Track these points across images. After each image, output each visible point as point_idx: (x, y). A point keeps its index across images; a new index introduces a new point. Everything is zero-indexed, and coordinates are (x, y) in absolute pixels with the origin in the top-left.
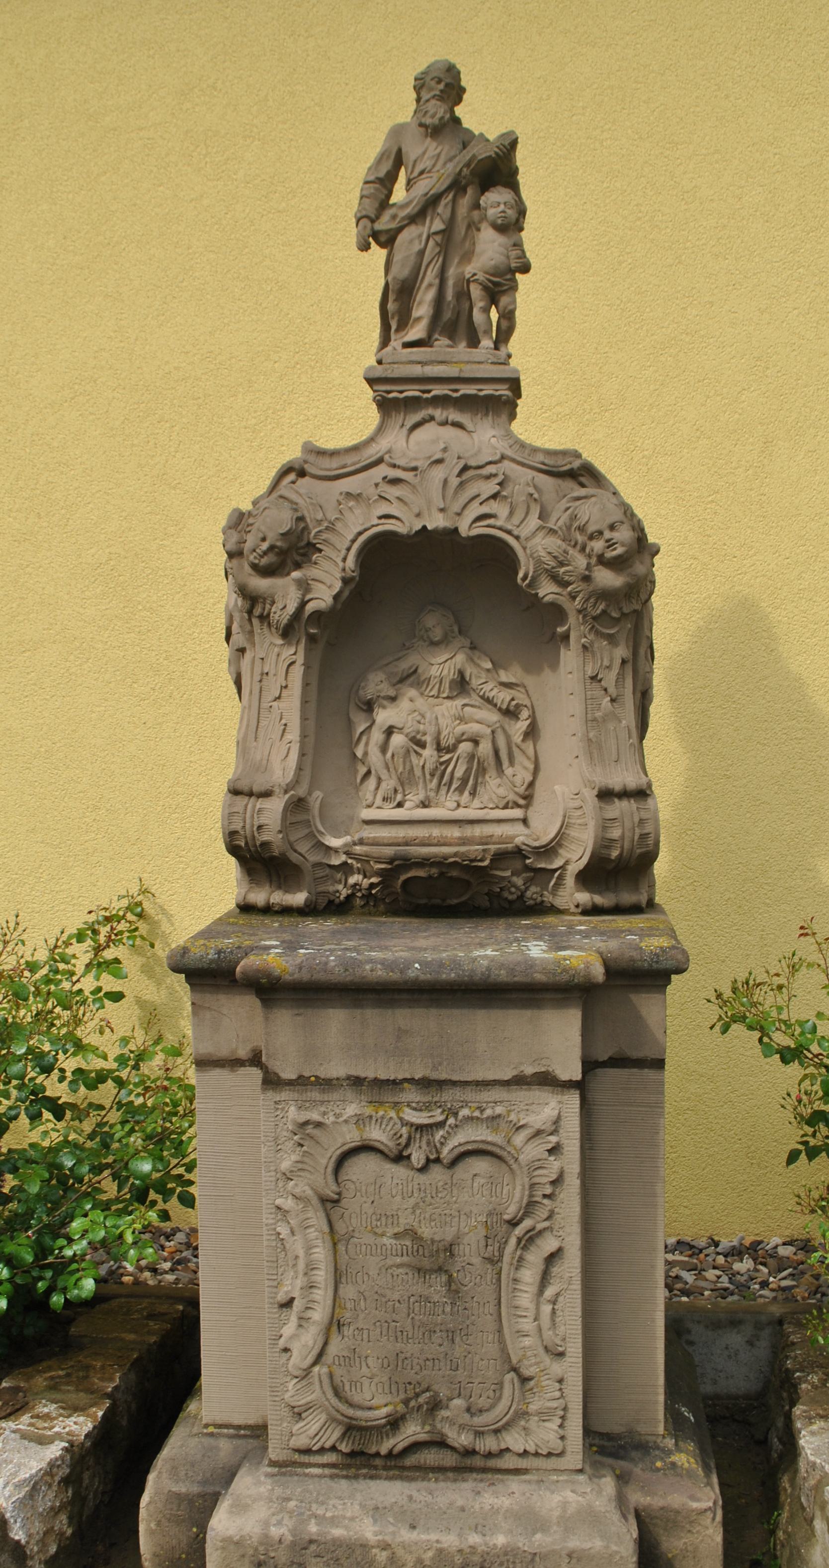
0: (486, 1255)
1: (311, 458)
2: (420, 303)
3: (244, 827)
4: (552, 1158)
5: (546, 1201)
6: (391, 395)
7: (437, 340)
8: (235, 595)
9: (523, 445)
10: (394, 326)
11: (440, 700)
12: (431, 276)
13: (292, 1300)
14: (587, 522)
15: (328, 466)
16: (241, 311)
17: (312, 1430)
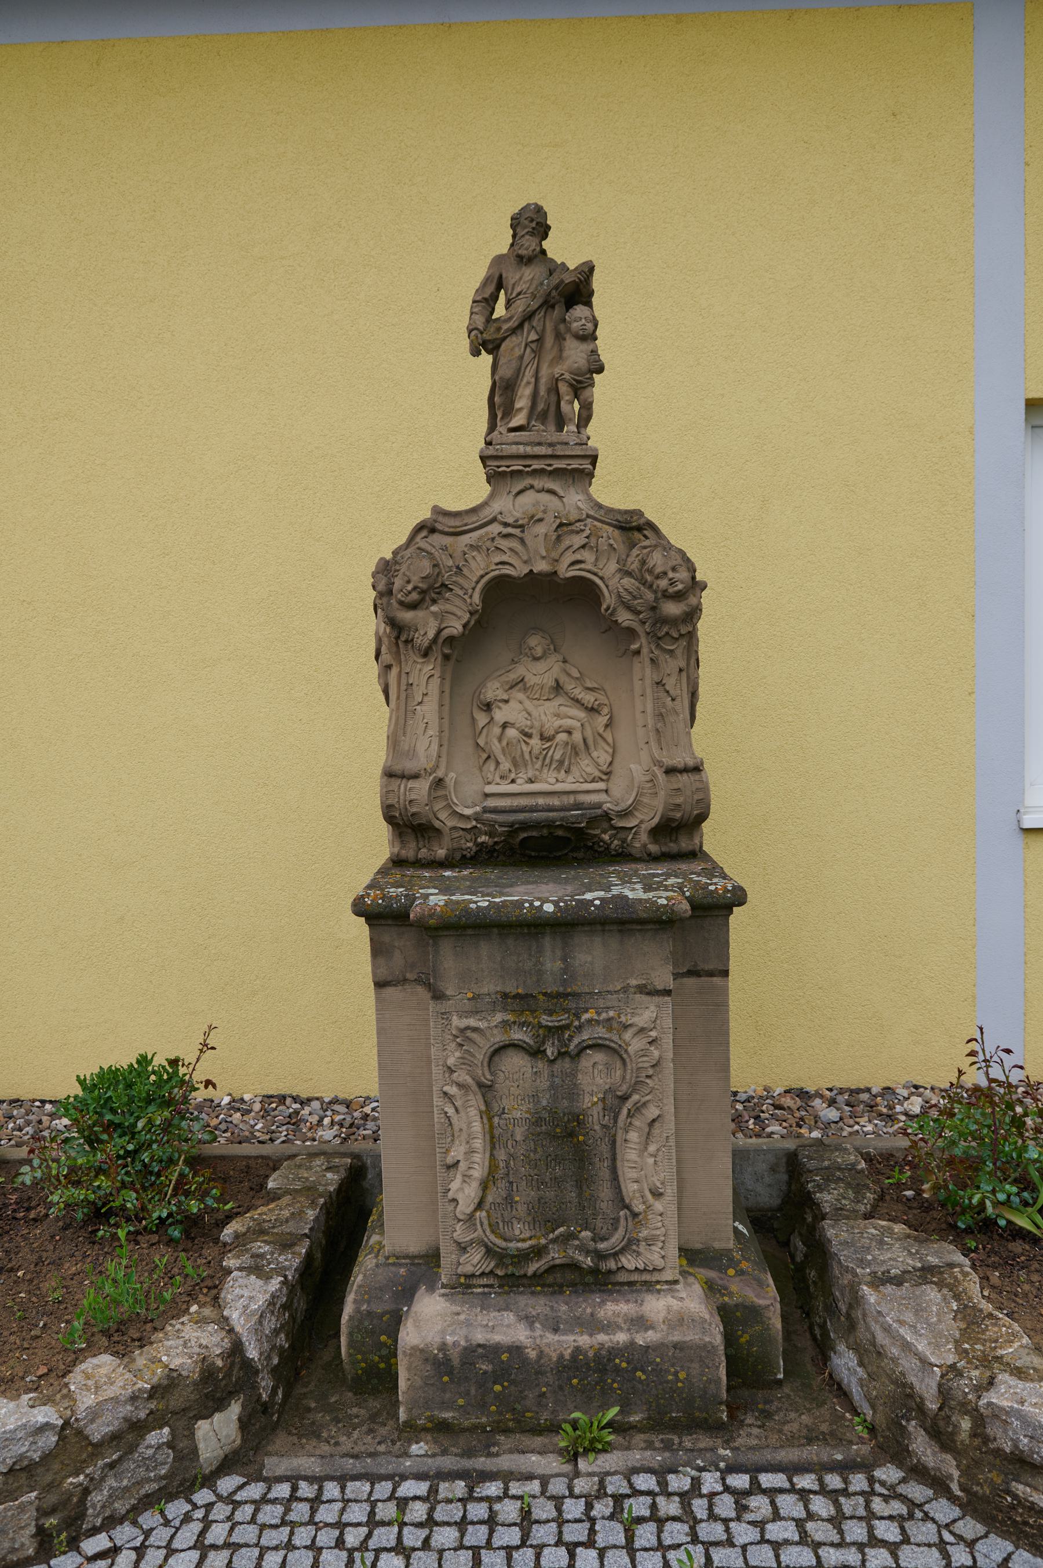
0: (604, 1123)
1: (440, 518)
3: (398, 802)
4: (652, 1048)
5: (648, 1081)
8: (383, 625)
9: (600, 506)
11: (541, 702)
12: (528, 375)
13: (458, 1161)
15: (453, 524)
17: (474, 1261)
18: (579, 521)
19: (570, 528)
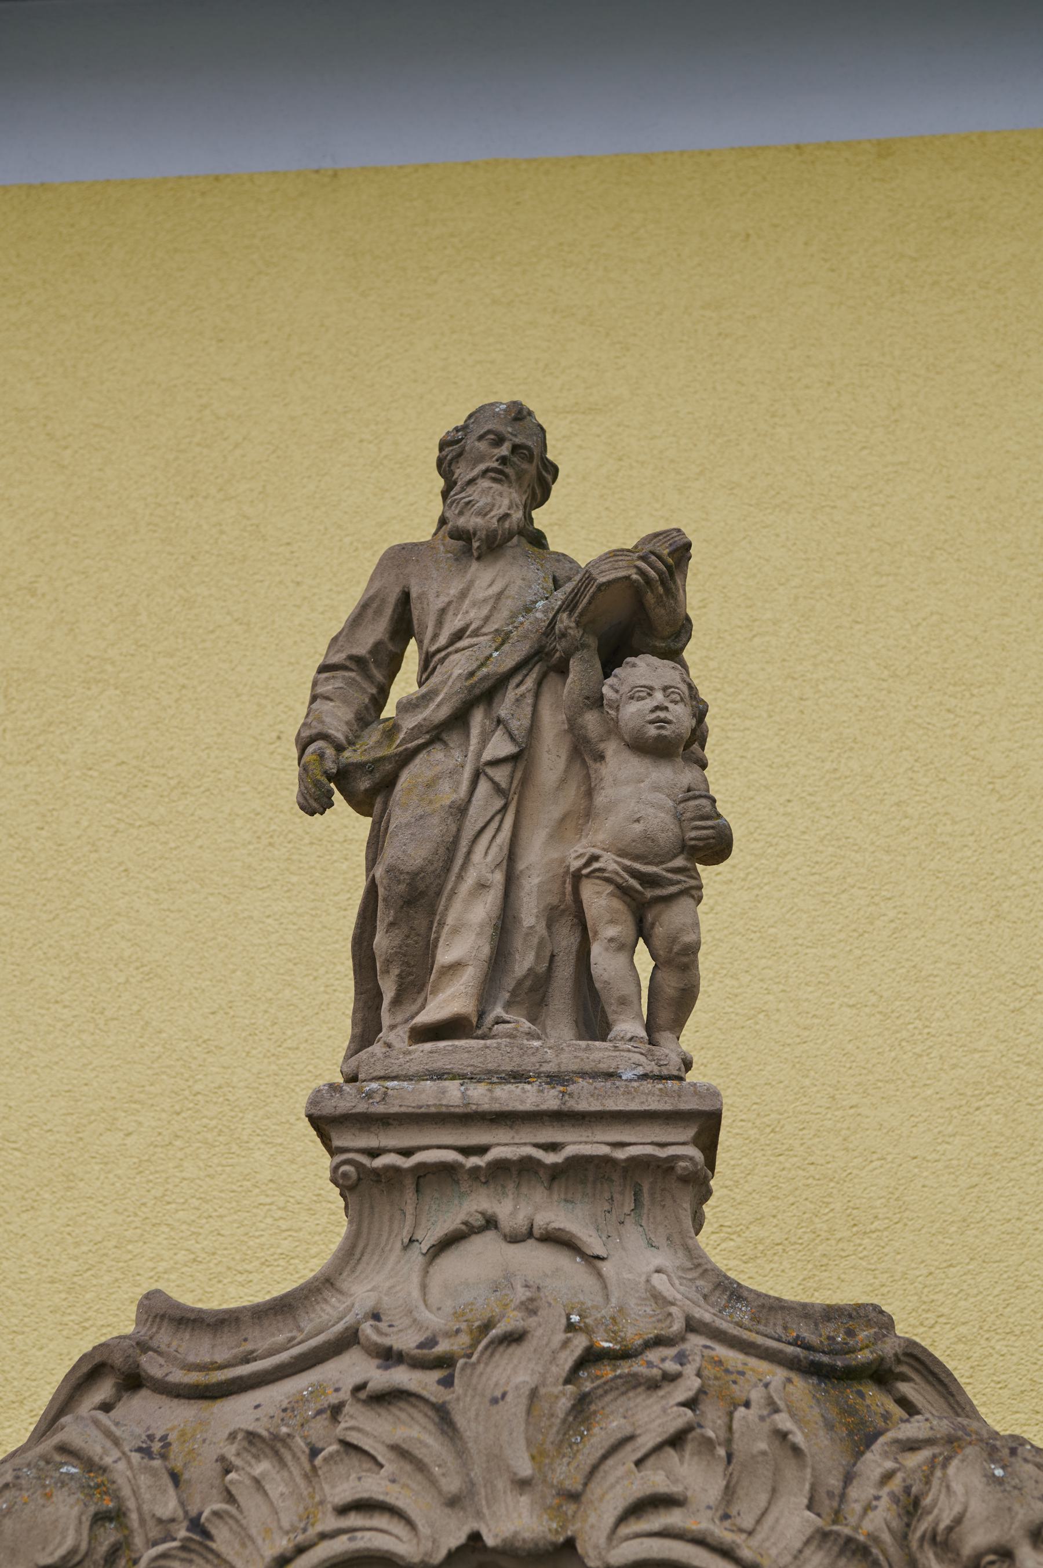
1: (164, 1338)
2: (455, 931)
6: (379, 1162)
7: (499, 1021)
9: (733, 1293)
10: (388, 989)
12: (484, 862)
14: (958, 1520)
16: (59, 1025)
18: (659, 1342)
19: (625, 1368)
